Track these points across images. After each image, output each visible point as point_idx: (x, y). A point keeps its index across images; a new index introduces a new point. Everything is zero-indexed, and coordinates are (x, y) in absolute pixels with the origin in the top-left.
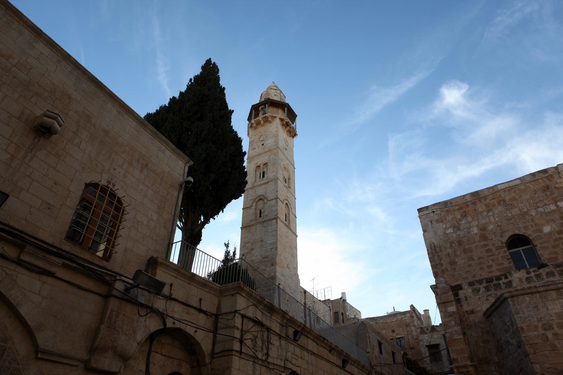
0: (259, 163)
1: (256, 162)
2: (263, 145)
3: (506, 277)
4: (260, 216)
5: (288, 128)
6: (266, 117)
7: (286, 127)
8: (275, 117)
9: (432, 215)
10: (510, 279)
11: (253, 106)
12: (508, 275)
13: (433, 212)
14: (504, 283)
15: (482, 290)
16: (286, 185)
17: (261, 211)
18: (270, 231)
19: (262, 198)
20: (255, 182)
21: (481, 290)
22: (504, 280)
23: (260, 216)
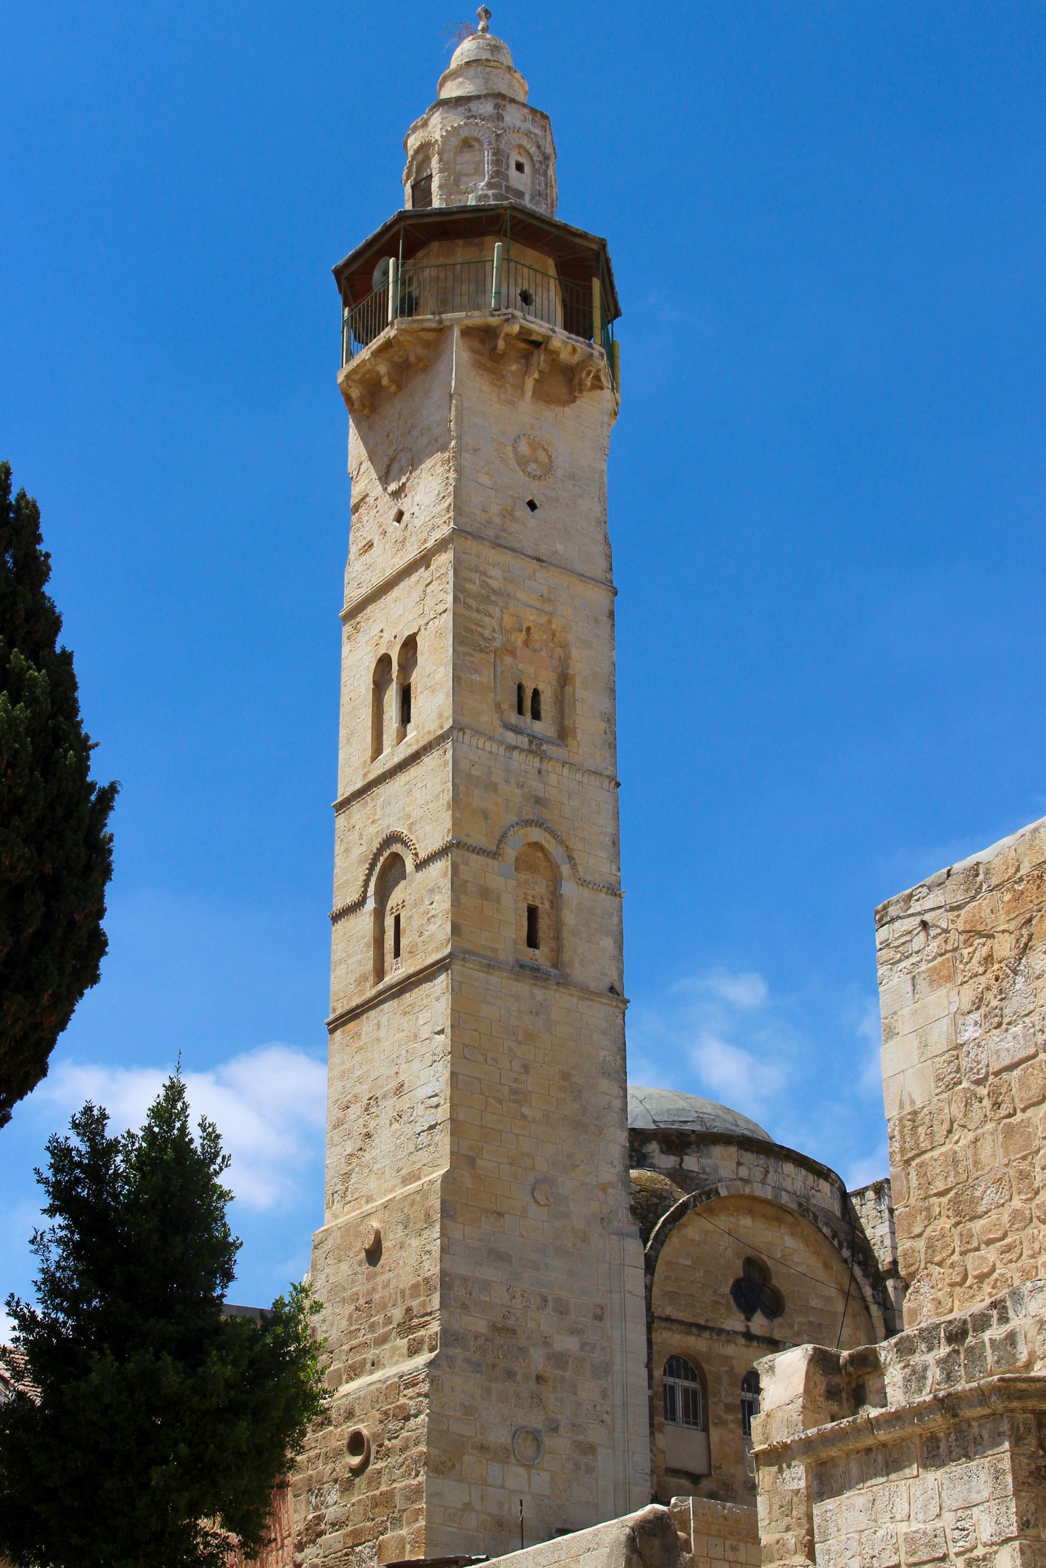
0: (388, 636)
1: (375, 631)
2: (399, 517)
3: (1004, 1319)
4: (397, 954)
5: (540, 359)
6: (388, 344)
7: (526, 357)
8: (442, 331)
9: (919, 941)
10: (1015, 1323)
11: (338, 273)
12: (1008, 1304)
13: (924, 925)
14: (992, 1341)
15: (934, 1374)
16: (543, 728)
17: (397, 919)
18: (425, 1032)
19: (397, 848)
20: (378, 751)
21: (929, 1374)
22: (995, 1332)
23: (397, 954)
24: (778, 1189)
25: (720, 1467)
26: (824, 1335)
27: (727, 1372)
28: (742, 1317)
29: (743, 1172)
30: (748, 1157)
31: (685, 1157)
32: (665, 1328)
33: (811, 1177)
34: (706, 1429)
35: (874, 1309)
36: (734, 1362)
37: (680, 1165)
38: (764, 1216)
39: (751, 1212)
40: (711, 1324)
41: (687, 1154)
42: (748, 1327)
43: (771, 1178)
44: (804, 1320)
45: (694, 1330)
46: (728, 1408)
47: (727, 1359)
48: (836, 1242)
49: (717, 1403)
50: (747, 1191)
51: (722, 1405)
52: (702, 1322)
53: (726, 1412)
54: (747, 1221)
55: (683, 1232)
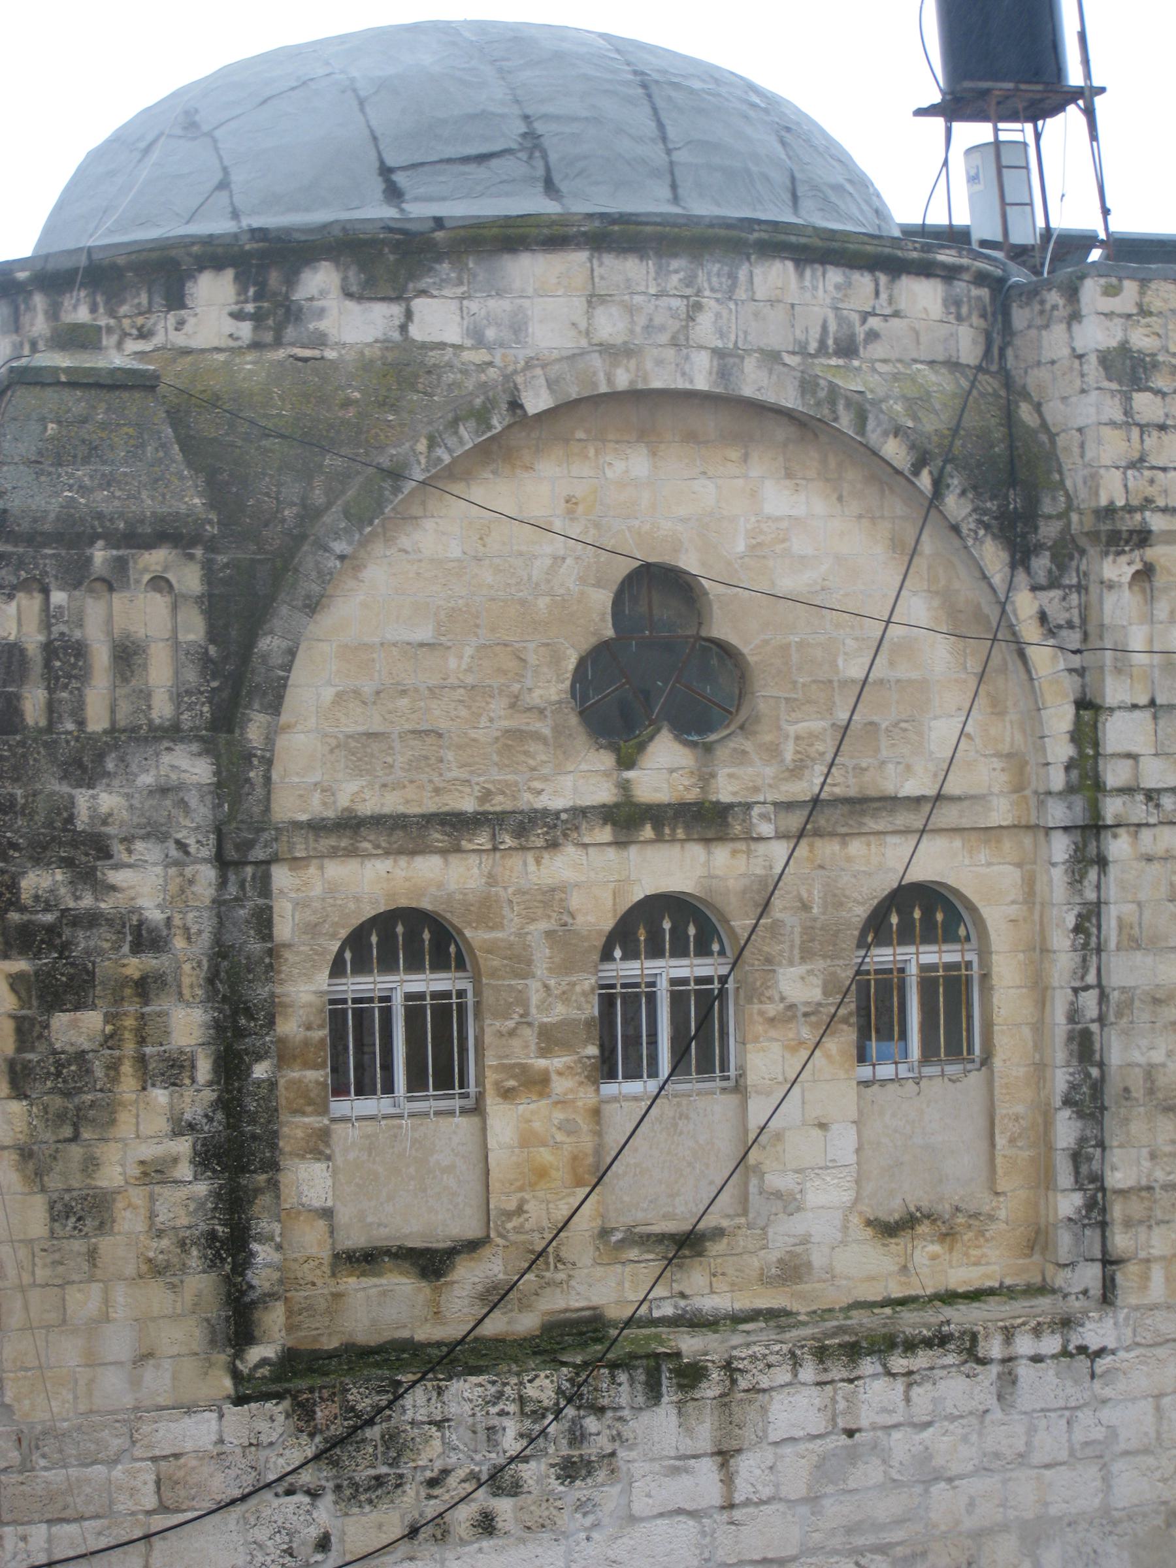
24: (726, 359)
25: (520, 1210)
26: (884, 753)
27: (549, 934)
28: (606, 760)
29: (610, 325)
30: (630, 271)
31: (418, 304)
32: (334, 853)
33: (863, 281)
34: (477, 1110)
35: (1045, 660)
36: (575, 901)
37: (403, 328)
38: (691, 437)
39: (646, 435)
40: (499, 804)
41: (423, 293)
42: (625, 787)
43: (705, 328)
44: (817, 725)
45: (437, 836)
46: (550, 1039)
47: (552, 898)
48: (925, 481)
49: (512, 1033)
50: (623, 380)
51: (530, 1035)
52: (468, 805)
53: (544, 1053)
54: (629, 466)
55: (404, 541)
